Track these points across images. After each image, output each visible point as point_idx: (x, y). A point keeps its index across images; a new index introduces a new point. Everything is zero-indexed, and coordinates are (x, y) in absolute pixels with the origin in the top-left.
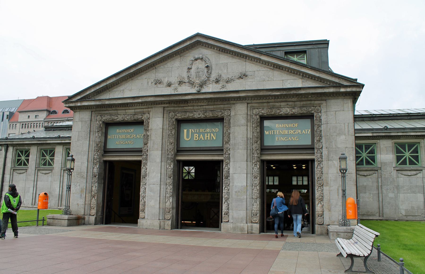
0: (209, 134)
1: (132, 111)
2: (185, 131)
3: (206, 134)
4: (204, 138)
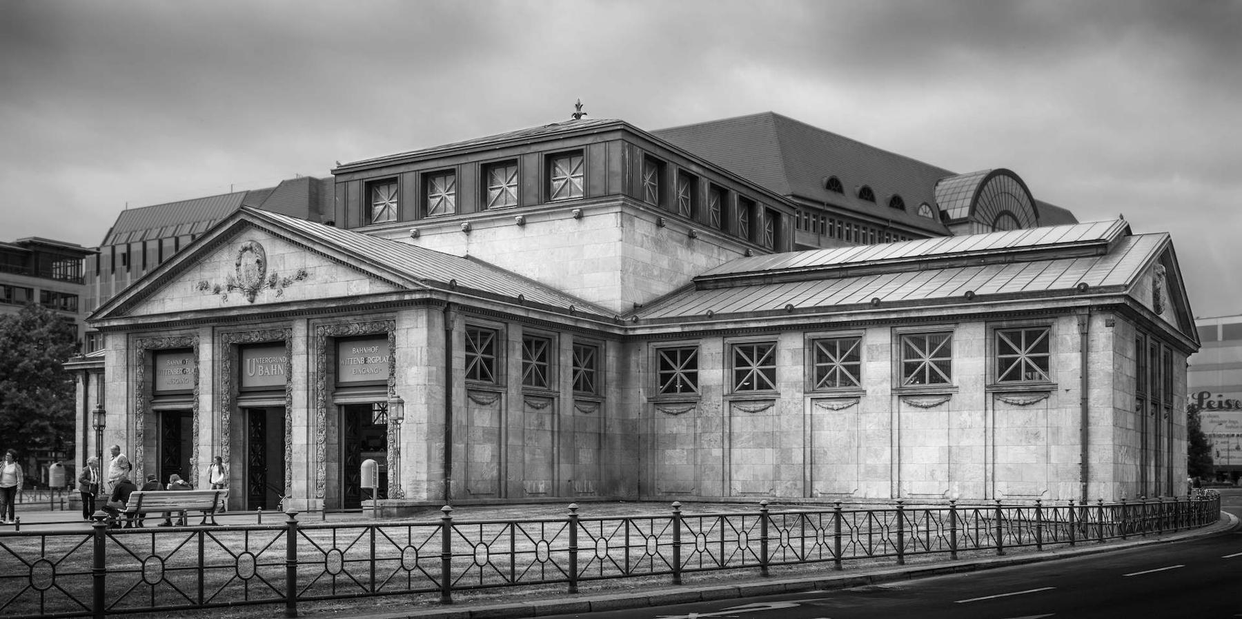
1: (176, 333)
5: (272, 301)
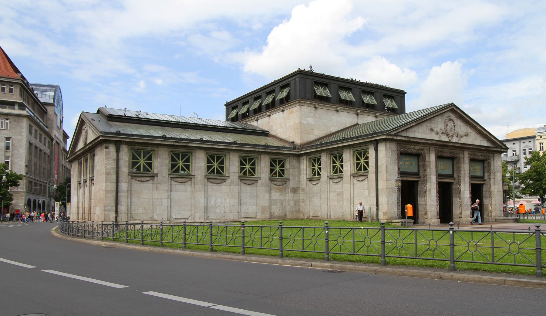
1: (417, 147)
5: (457, 142)
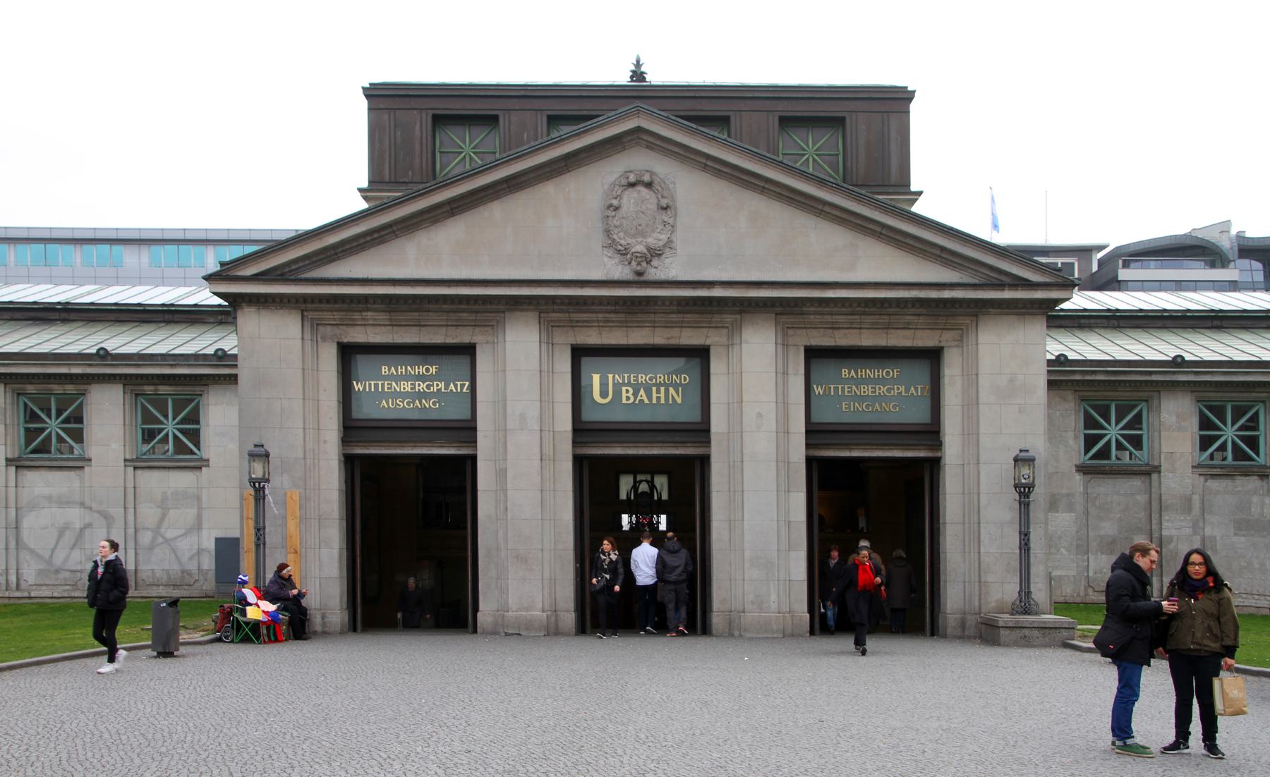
0: (662, 389)
2: (596, 378)
3: (654, 389)
4: (650, 398)
